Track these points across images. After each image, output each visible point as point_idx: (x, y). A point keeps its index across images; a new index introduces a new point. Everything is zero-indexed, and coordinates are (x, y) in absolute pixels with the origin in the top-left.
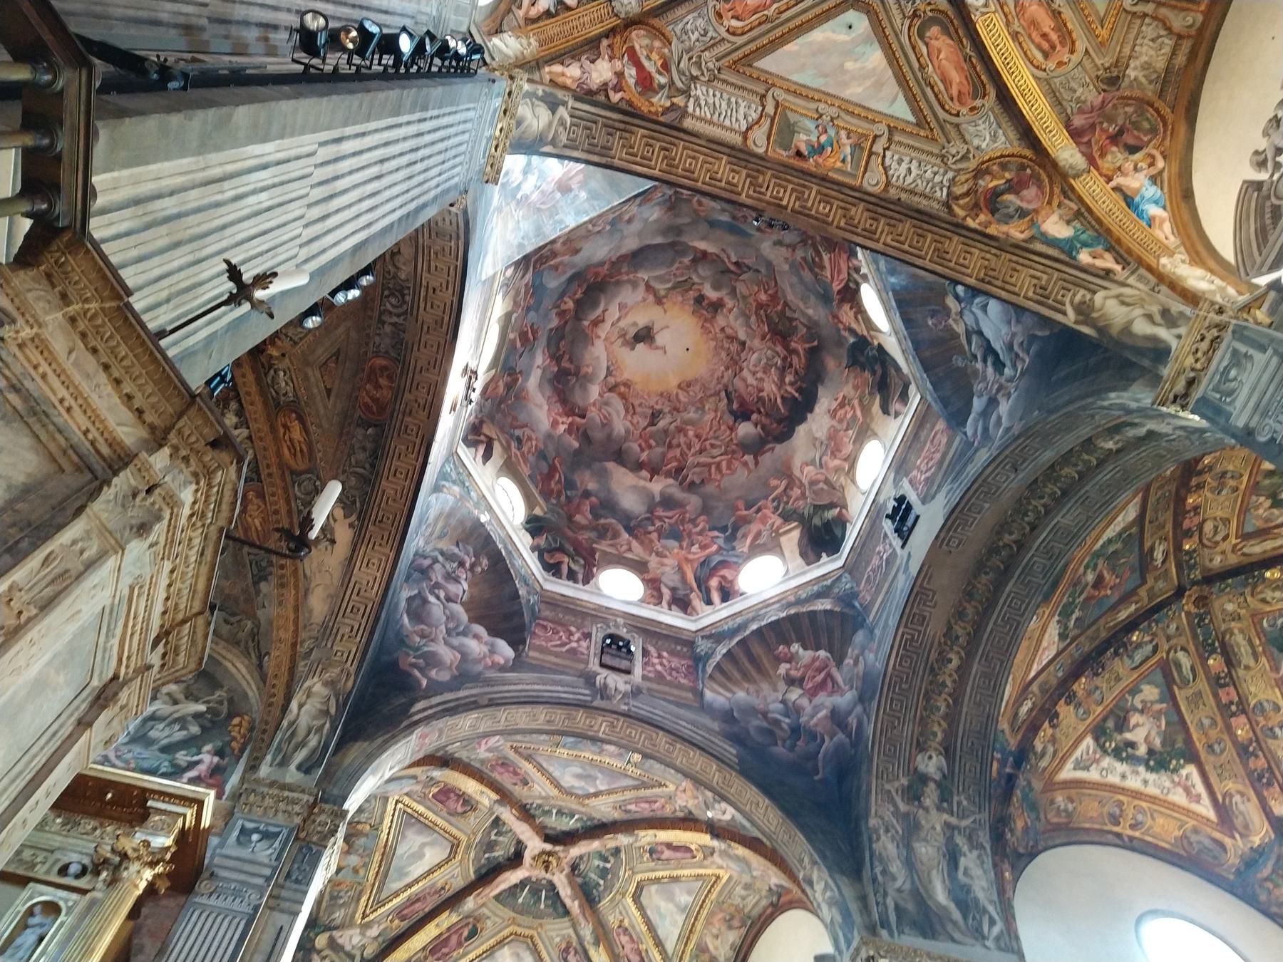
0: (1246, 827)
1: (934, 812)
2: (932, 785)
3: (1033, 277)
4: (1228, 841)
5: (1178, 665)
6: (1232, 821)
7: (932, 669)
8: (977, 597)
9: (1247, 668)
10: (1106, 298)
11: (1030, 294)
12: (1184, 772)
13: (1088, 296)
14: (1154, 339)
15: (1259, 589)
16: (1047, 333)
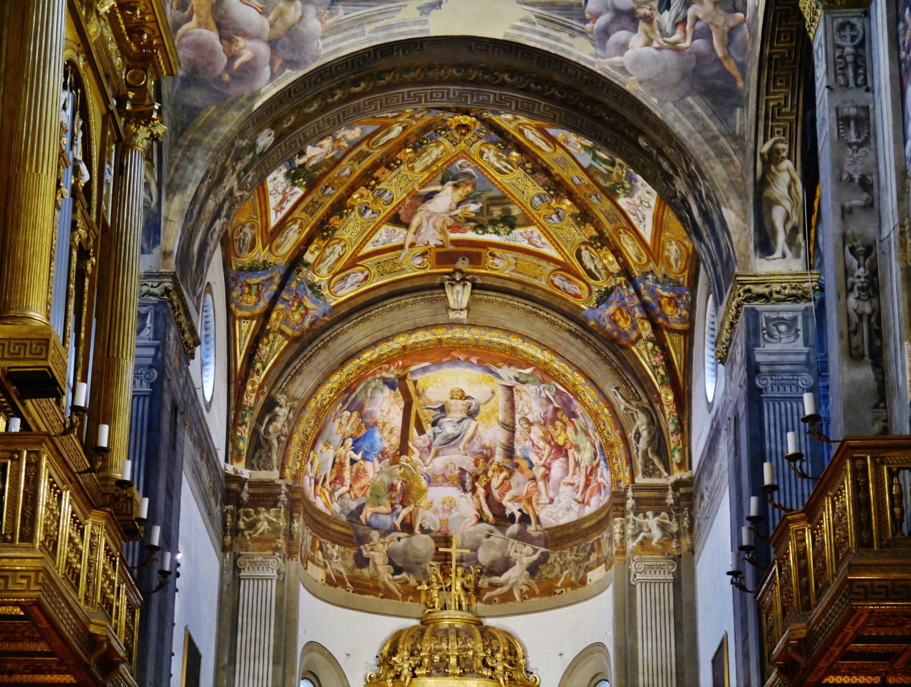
0: (278, 247)
1: (235, 176)
2: (251, 156)
3: (786, 99)
4: (259, 245)
5: (387, 133)
6: (276, 238)
7: (343, 83)
8: (431, 74)
9: (412, 169)
10: (788, 170)
11: (771, 104)
12: (296, 189)
13: (785, 154)
14: (774, 232)
15: (491, 146)
16: (720, 54)
